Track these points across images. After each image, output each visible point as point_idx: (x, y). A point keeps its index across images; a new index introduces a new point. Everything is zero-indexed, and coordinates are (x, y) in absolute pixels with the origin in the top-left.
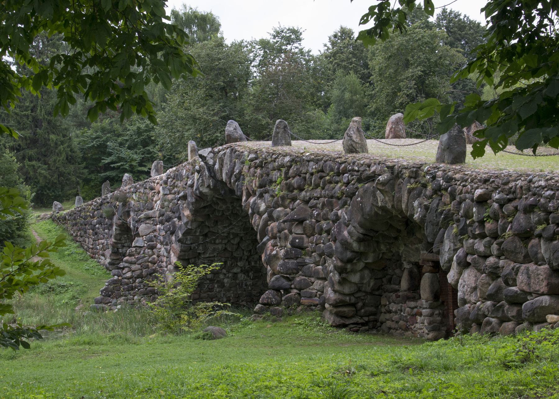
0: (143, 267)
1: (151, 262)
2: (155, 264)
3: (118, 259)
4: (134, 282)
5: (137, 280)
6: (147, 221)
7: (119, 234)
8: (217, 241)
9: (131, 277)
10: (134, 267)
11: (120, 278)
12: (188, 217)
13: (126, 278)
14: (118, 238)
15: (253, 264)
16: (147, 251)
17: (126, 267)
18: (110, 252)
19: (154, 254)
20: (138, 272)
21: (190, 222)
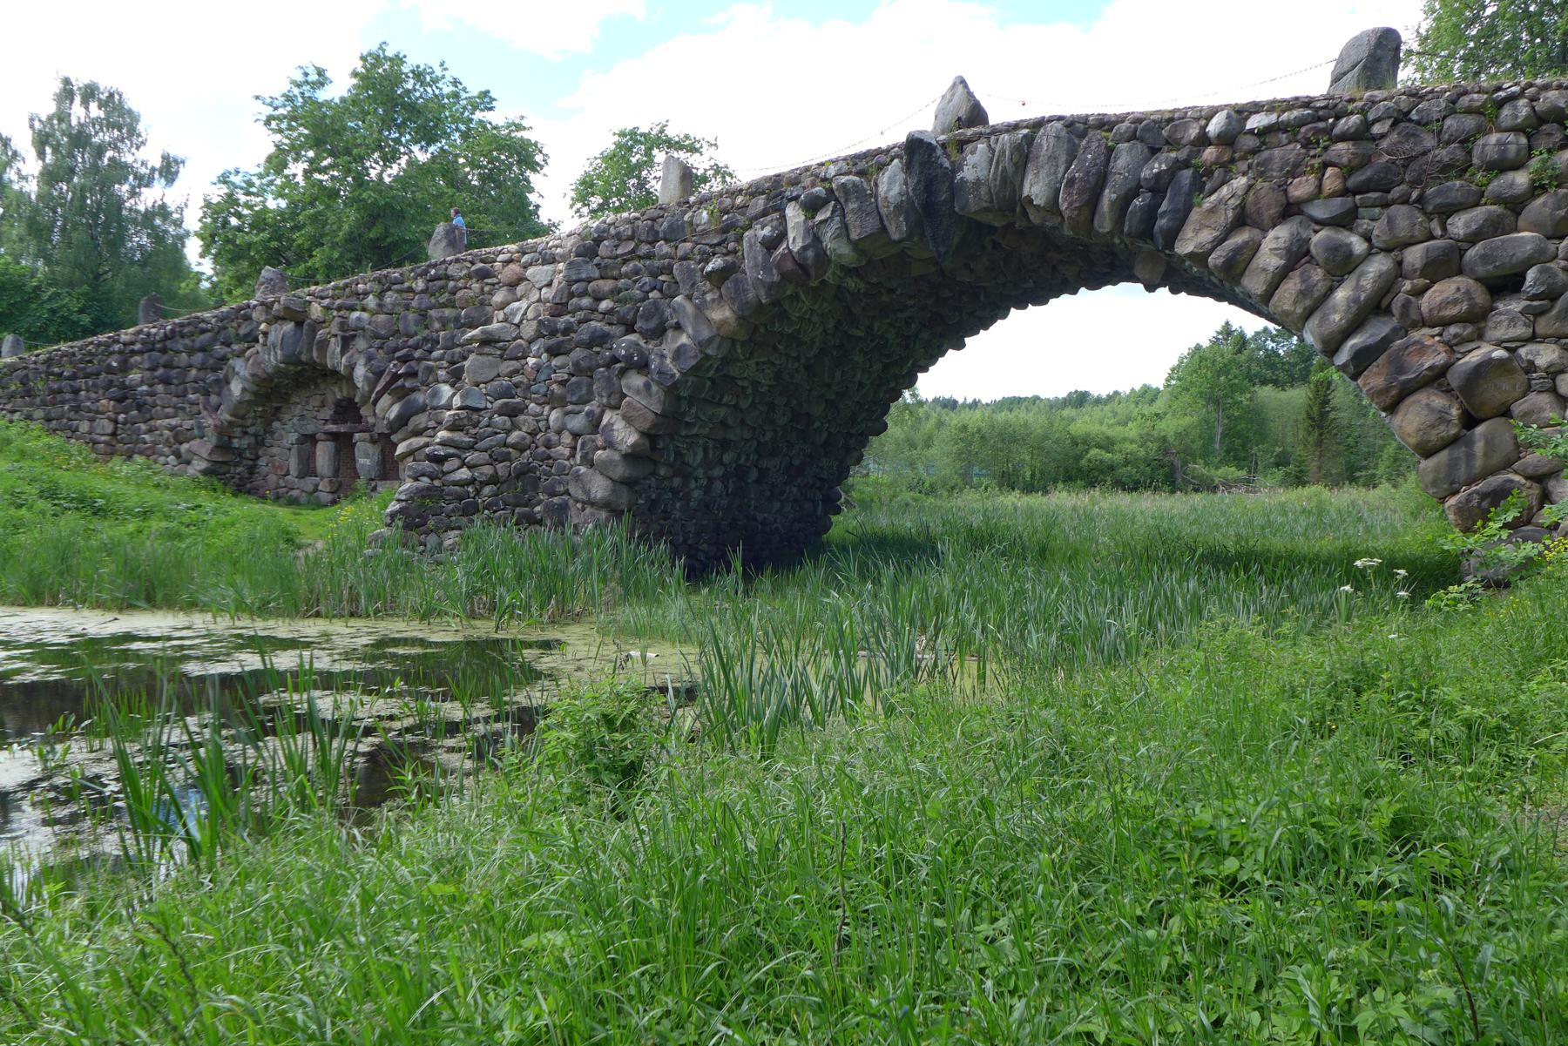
0: (494, 460)
1: (514, 446)
2: (522, 451)
3: (225, 463)
4: (478, 492)
5: (487, 490)
6: (487, 350)
7: (249, 402)
8: (725, 400)
9: (472, 481)
10: (471, 457)
11: (437, 483)
12: (723, 323)
13: (455, 483)
14: (242, 412)
15: (742, 461)
16: (497, 418)
17: (453, 456)
18: (210, 446)
19: (515, 427)
20: (488, 470)
21: (718, 340)
